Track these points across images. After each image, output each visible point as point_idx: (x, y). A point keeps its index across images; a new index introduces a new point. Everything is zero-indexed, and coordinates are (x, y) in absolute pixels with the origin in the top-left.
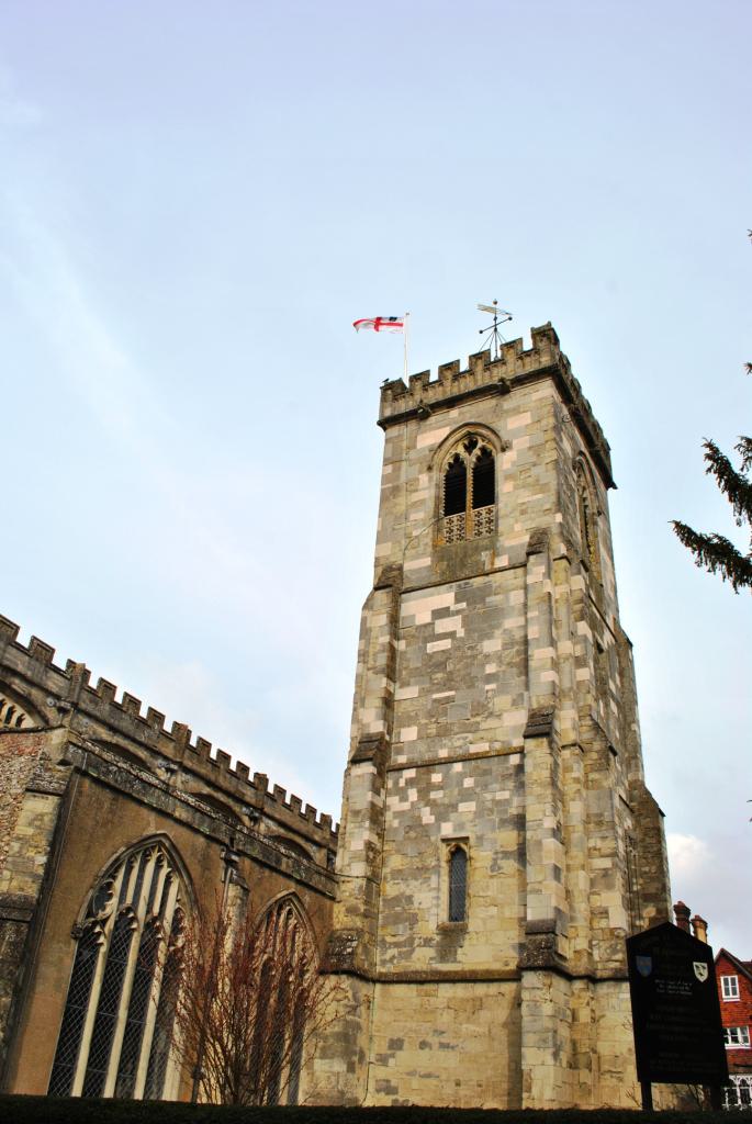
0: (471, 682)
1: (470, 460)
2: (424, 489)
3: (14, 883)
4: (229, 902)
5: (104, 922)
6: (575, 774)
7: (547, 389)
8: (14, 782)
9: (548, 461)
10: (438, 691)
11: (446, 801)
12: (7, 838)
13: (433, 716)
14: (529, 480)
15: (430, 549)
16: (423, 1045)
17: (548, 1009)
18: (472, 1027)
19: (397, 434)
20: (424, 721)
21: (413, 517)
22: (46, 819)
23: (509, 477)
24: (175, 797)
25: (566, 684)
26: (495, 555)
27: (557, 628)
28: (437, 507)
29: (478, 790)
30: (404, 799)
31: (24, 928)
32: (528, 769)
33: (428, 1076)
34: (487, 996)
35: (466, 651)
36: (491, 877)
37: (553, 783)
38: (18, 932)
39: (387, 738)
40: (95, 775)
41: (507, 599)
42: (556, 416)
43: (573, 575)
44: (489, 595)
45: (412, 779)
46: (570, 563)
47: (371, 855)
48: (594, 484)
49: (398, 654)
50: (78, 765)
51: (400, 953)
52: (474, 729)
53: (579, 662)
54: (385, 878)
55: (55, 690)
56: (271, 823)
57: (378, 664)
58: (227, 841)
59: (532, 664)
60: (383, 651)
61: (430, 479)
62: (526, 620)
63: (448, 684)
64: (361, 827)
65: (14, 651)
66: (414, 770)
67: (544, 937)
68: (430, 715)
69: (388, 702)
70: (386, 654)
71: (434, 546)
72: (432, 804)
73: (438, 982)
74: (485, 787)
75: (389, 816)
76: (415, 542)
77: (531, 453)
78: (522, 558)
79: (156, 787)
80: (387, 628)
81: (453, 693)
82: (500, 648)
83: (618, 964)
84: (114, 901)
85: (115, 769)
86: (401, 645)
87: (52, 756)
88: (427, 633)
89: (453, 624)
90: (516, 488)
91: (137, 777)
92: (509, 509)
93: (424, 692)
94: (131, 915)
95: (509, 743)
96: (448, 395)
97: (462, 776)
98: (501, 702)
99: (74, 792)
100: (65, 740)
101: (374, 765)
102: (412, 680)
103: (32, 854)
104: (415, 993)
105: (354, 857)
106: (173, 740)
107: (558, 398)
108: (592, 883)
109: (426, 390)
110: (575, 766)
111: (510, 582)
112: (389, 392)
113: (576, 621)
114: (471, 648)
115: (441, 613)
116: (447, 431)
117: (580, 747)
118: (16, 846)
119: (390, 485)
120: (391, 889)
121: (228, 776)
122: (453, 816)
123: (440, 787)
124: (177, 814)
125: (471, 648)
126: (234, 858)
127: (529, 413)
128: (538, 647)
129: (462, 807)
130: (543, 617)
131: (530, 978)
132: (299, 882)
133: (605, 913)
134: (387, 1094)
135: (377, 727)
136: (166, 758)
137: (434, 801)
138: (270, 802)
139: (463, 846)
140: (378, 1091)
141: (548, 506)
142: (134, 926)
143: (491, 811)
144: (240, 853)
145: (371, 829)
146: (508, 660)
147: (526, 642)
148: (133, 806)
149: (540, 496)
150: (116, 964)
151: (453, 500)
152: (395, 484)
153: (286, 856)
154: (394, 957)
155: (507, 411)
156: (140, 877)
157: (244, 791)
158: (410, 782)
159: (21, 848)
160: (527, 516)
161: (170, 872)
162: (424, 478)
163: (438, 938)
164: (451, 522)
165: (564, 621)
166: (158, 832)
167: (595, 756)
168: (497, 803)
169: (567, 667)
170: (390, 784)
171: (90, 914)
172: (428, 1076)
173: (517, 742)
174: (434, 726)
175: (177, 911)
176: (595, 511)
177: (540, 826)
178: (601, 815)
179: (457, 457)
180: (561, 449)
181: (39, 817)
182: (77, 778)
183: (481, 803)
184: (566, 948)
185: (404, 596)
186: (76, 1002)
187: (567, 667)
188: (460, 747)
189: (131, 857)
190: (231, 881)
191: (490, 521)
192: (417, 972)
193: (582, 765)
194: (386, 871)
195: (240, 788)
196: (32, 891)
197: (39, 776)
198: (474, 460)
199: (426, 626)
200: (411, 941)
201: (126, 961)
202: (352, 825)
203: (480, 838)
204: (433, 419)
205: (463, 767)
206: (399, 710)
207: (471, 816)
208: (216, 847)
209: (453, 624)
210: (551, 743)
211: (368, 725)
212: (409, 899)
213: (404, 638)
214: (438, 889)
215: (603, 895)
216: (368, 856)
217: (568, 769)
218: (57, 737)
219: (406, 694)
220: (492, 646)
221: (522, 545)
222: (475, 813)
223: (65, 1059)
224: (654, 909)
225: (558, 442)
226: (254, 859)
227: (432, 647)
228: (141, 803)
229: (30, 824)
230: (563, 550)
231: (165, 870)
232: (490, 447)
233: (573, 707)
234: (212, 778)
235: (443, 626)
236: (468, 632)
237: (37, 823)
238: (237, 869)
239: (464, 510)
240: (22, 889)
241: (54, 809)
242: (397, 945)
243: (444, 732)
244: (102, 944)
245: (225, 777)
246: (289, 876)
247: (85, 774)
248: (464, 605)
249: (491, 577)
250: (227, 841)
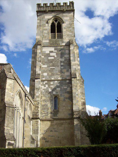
13: (50, 71)
18: (61, 128)
23: (65, 28)
30: (45, 86)
33: (53, 136)
41: (65, 52)
45: (46, 83)
63: (53, 66)
74: (62, 86)
77: (69, 25)
82: (64, 60)
88: (48, 55)
89: (54, 54)
93: (49, 67)
115: (51, 52)
129: (57, 89)
137: (51, 87)
141: (73, 36)
146: (65, 63)
149: (71, 33)
151: (53, 30)
158: (46, 84)
165: (76, 57)
168: (64, 89)
172: (53, 136)
178: (83, 92)
181: (11, 84)
183: (61, 89)
199: (48, 54)
203: (61, 95)
209: (54, 54)
227: (50, 58)
232: (60, 22)
236: (57, 56)
242: (44, 113)
243: (53, 75)
248: (56, 51)
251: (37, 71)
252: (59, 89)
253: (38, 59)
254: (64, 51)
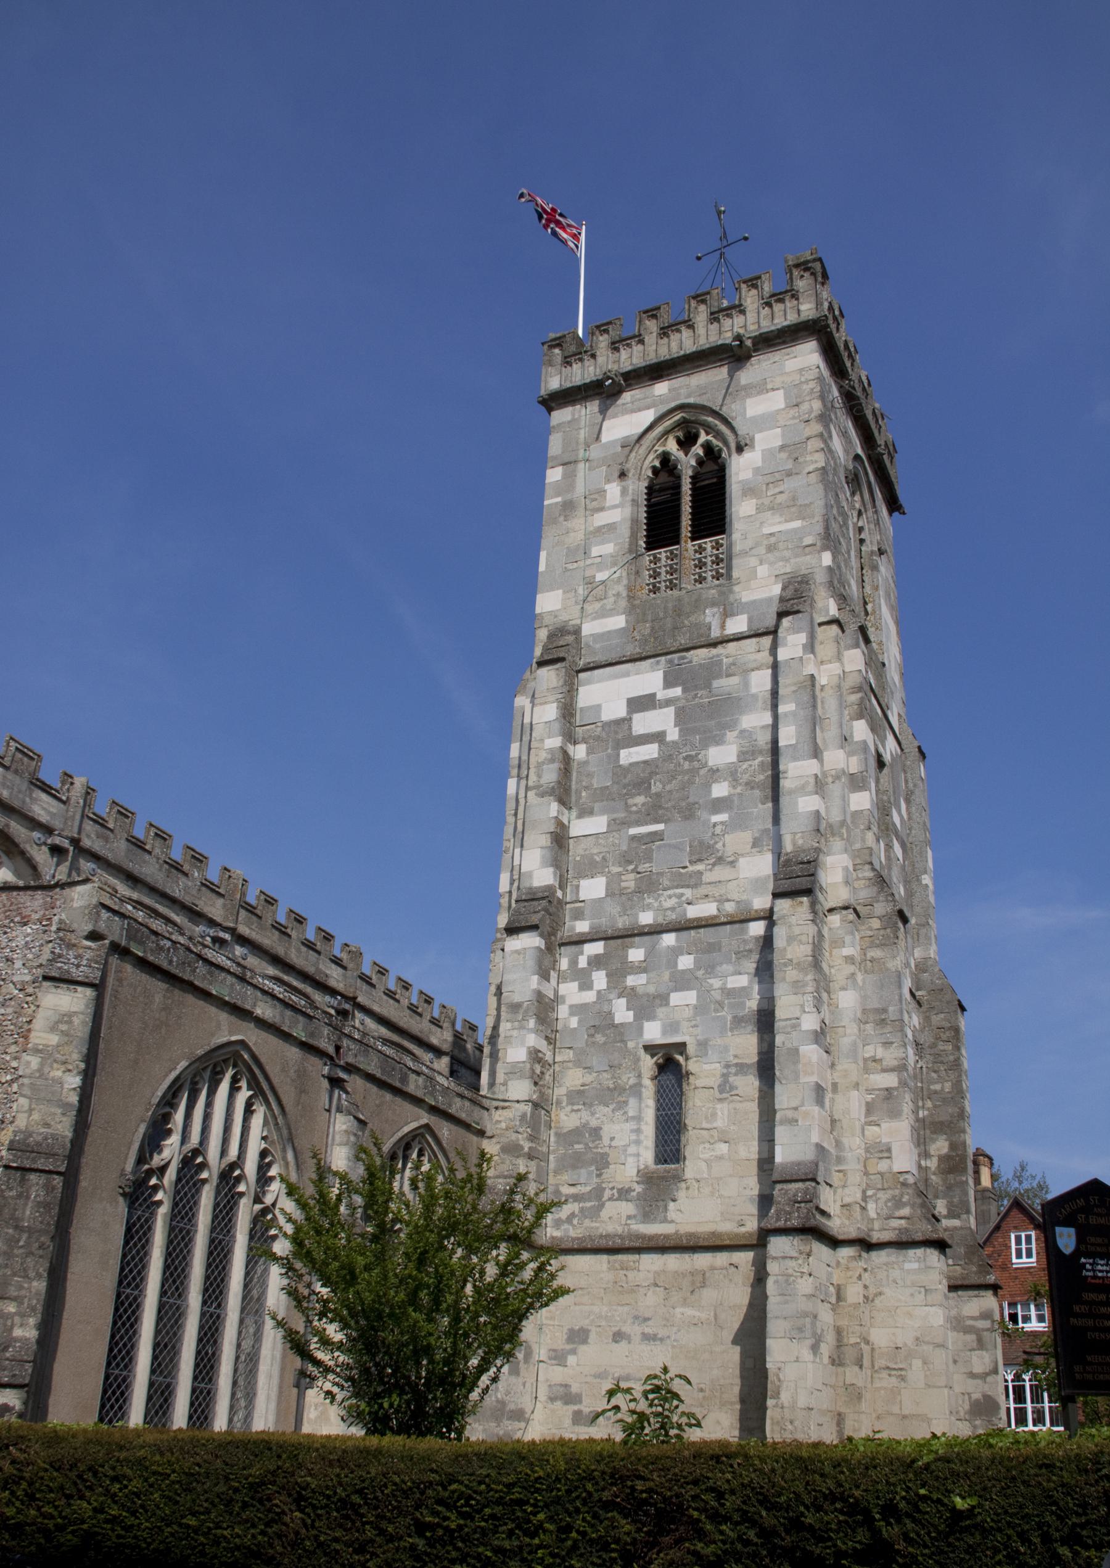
0: (689, 813)
1: (687, 463)
2: (615, 507)
3: (36, 1116)
4: (338, 1138)
5: (163, 1169)
6: (847, 951)
7: (807, 356)
8: (18, 964)
9: (811, 468)
10: (638, 823)
11: (651, 989)
12: (13, 1049)
13: (630, 862)
14: (780, 499)
15: (623, 603)
16: (618, 1336)
17: (805, 1286)
18: (689, 1312)
19: (569, 418)
20: (616, 869)
21: (595, 551)
22: (76, 1021)
23: (749, 491)
24: (255, 987)
25: (835, 816)
26: (727, 614)
27: (822, 730)
28: (634, 536)
29: (700, 973)
30: (586, 985)
31: (58, 1181)
32: (779, 942)
34: (713, 1268)
35: (680, 766)
36: (720, 1100)
37: (816, 964)
38: (49, 1188)
39: (559, 894)
40: (140, 954)
41: (746, 684)
42: (822, 398)
43: (848, 648)
44: (719, 676)
46: (843, 631)
47: (538, 1069)
48: (874, 506)
49: (575, 766)
50: (116, 938)
51: (582, 1210)
52: (695, 881)
53: (856, 783)
54: (559, 1102)
55: (43, 817)
56: (368, 1021)
57: (543, 781)
58: (331, 1050)
59: (785, 784)
60: (552, 761)
61: (624, 492)
62: (776, 717)
63: (652, 814)
64: (522, 1028)
66: (602, 943)
67: (800, 1185)
68: (625, 860)
69: (560, 838)
70: (555, 766)
71: (630, 598)
72: (631, 995)
73: (639, 1250)
74: (711, 969)
75: (563, 1011)
76: (599, 591)
77: (784, 455)
78: (770, 621)
79: (228, 972)
80: (557, 726)
81: (660, 827)
82: (734, 759)
83: (903, 1221)
84: (174, 1139)
85: (169, 944)
86: (579, 752)
87: (75, 926)
88: (619, 733)
89: (662, 720)
90: (759, 510)
91: (200, 956)
92: (749, 543)
93: (616, 825)
94: (199, 1160)
95: (748, 903)
96: (652, 359)
97: (676, 952)
98: (736, 841)
99: (111, 981)
100: (94, 901)
101: (541, 935)
102: (597, 806)
103: (59, 1073)
104: (605, 1266)
105: (514, 1071)
106: (222, 896)
107: (826, 373)
108: (870, 1108)
109: (617, 350)
110: (848, 939)
111: (752, 657)
112: (557, 351)
113: (852, 719)
114: (688, 758)
115: (642, 703)
116: (649, 416)
117: (855, 910)
118: (34, 1062)
119: (559, 499)
120: (567, 1119)
121: (304, 949)
122: (661, 1012)
123: (640, 968)
124: (258, 1011)
125: (688, 758)
126: (342, 1075)
127: (781, 392)
128: (795, 759)
130: (802, 712)
131: (778, 1245)
132: (434, 1110)
133: (886, 1152)
134: (566, 1403)
135: (543, 877)
136: (212, 923)
137: (633, 989)
138: (365, 987)
139: (680, 1058)
140: (552, 1399)
141: (808, 540)
142: (204, 1175)
143: (720, 1004)
144: (350, 1068)
145: (537, 1031)
146: (746, 777)
147: (775, 749)
148: (190, 999)
149: (797, 524)
150: (181, 1231)
151: (659, 528)
152: (569, 497)
153: (414, 1071)
154: (573, 1215)
155: (745, 388)
156: (209, 1104)
157: (328, 972)
158: (596, 962)
159: (42, 1065)
160: (777, 554)
161: (250, 1097)
162: (613, 490)
163: (639, 1189)
164: (656, 560)
166: (233, 1038)
167: (876, 924)
168: (729, 993)
169: (836, 789)
170: (564, 964)
171: (141, 1160)
173: (761, 902)
174: (632, 876)
175: (263, 1154)
176: (875, 549)
177: (795, 1027)
178: (885, 1010)
179: (665, 458)
180: (831, 451)
181: (67, 1017)
182: (114, 960)
183: (704, 993)
184: (828, 1200)
185: (582, 675)
186: (129, 1284)
187: (836, 789)
188: (673, 909)
189: (195, 1076)
190: (339, 1110)
191: (718, 561)
192: (607, 1236)
193: (858, 937)
194: (560, 1092)
195: (321, 966)
196: (64, 1127)
197: (60, 956)
198: (693, 463)
200: (598, 1192)
201: (195, 1225)
202: (509, 1025)
203: (703, 1045)
204: (627, 397)
205: (677, 940)
206: (576, 851)
207: (688, 1013)
208: (315, 1061)
209: (662, 720)
210: (813, 904)
211: (530, 874)
212: (596, 1132)
213: (584, 741)
214: (638, 1118)
215: (884, 1125)
216: (533, 1071)
217: (838, 943)
218: (81, 897)
219: (587, 826)
220: (723, 755)
221: (770, 600)
222: (695, 1007)
223: (118, 1365)
224: (946, 1144)
225: (825, 438)
226: (370, 1078)
227: (630, 756)
228: (205, 995)
229: (53, 1029)
230: (833, 610)
231: (244, 1094)
233: (846, 850)
234: (280, 951)
235: (643, 723)
237: (64, 1027)
238: (347, 1093)
239: (678, 543)
240: (47, 1125)
241: (87, 1006)
242: (577, 1198)
243: (648, 885)
244: (159, 1203)
245: (299, 951)
246: (417, 1101)
248: (677, 691)
249: (719, 650)
250: (331, 1050)
251: (544, 864)
252: (690, 997)
253: (539, 776)
254: (735, 680)
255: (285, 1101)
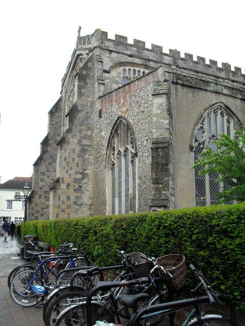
65: (146, 52)
91: (201, 80)
118: (155, 119)
124: (224, 92)
159: (157, 119)
181: (161, 105)
182: (173, 87)
218: (160, 72)
231: (226, 117)
247: (177, 83)
255: (239, 117)
